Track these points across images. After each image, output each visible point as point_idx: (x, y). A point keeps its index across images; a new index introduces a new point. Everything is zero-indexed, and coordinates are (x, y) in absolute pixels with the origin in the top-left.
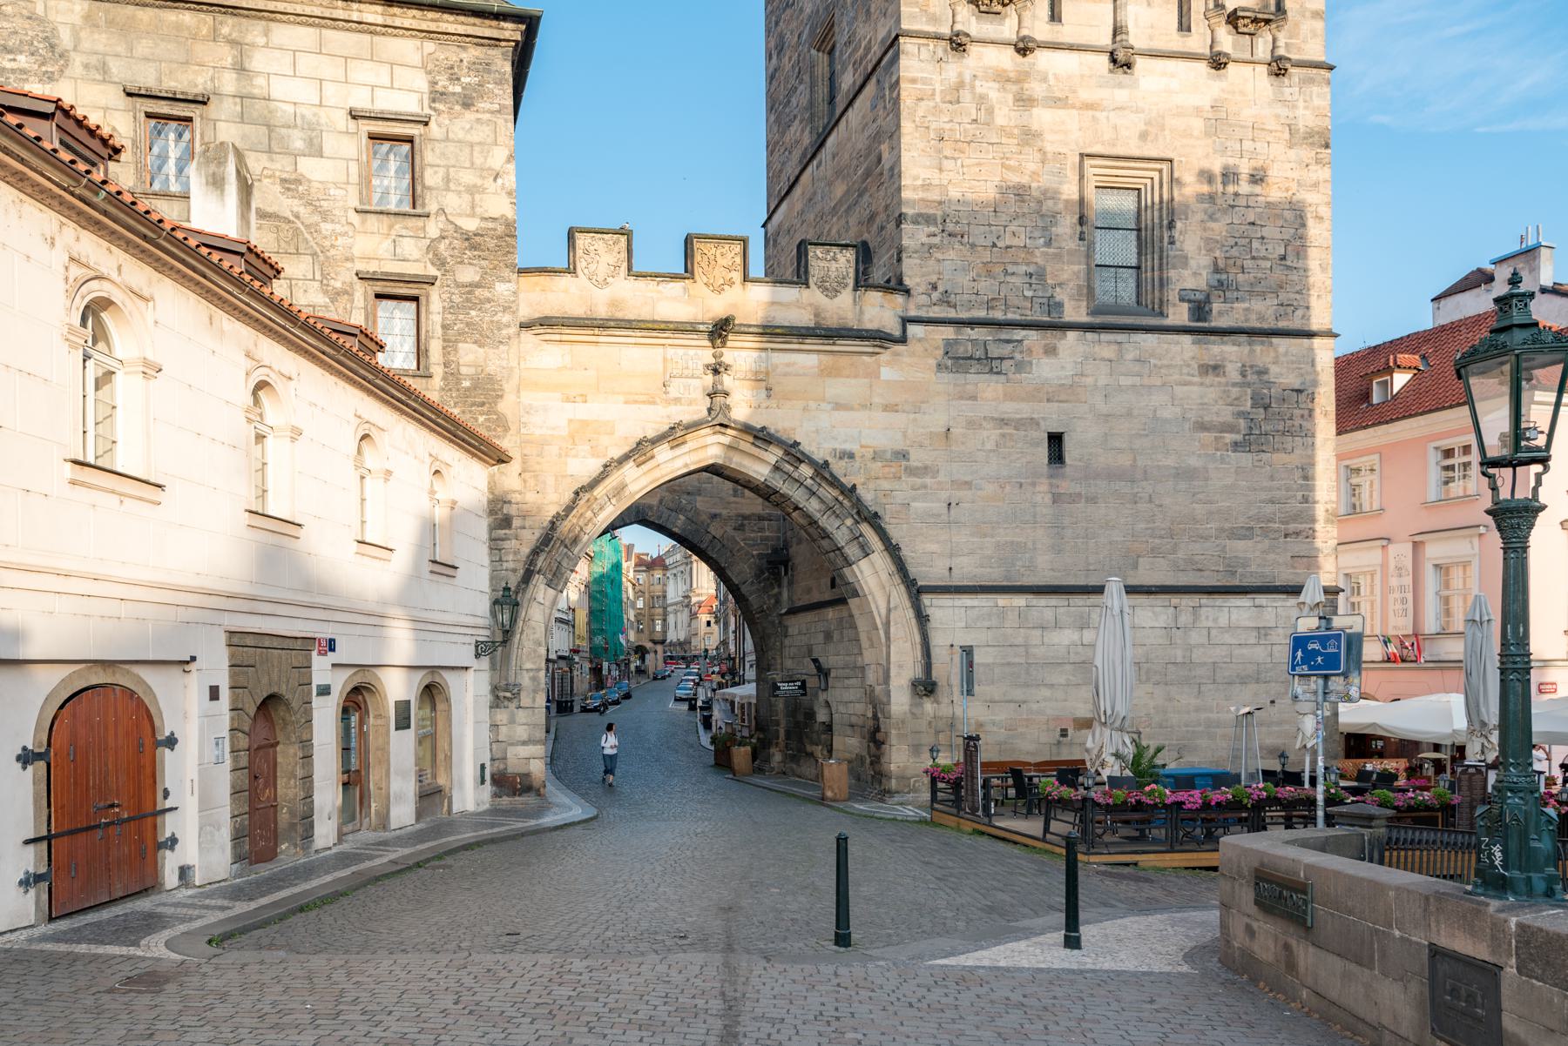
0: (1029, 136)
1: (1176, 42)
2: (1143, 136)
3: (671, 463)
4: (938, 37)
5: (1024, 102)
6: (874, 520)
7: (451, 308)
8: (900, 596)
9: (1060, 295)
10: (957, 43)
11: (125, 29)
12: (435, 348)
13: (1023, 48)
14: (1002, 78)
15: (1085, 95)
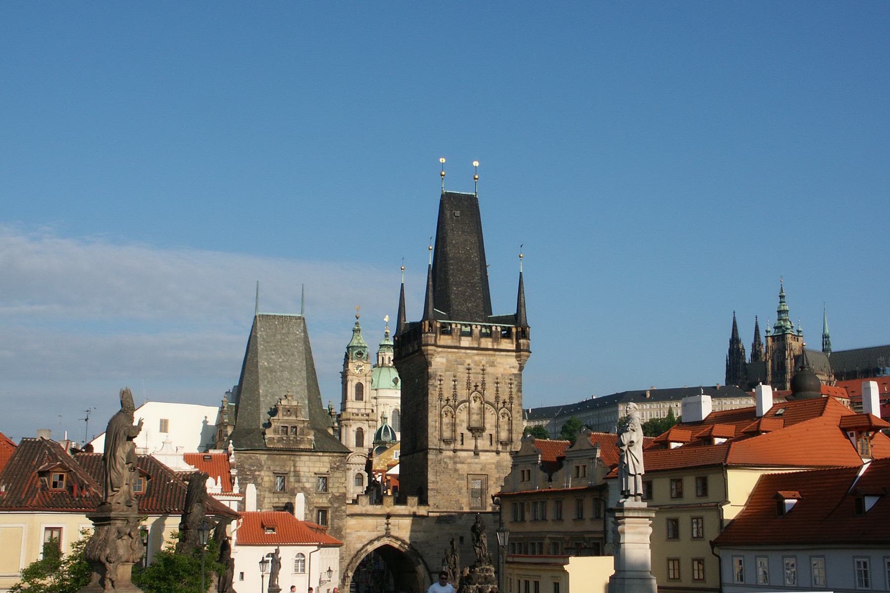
0: (456, 470)
1: (488, 448)
2: (481, 470)
3: (377, 544)
4: (436, 449)
5: (455, 463)
6: (421, 557)
7: (333, 512)
8: (427, 575)
9: (463, 505)
10: (440, 451)
11: (274, 460)
12: (329, 523)
13: (455, 451)
14: (450, 458)
15: (469, 461)
